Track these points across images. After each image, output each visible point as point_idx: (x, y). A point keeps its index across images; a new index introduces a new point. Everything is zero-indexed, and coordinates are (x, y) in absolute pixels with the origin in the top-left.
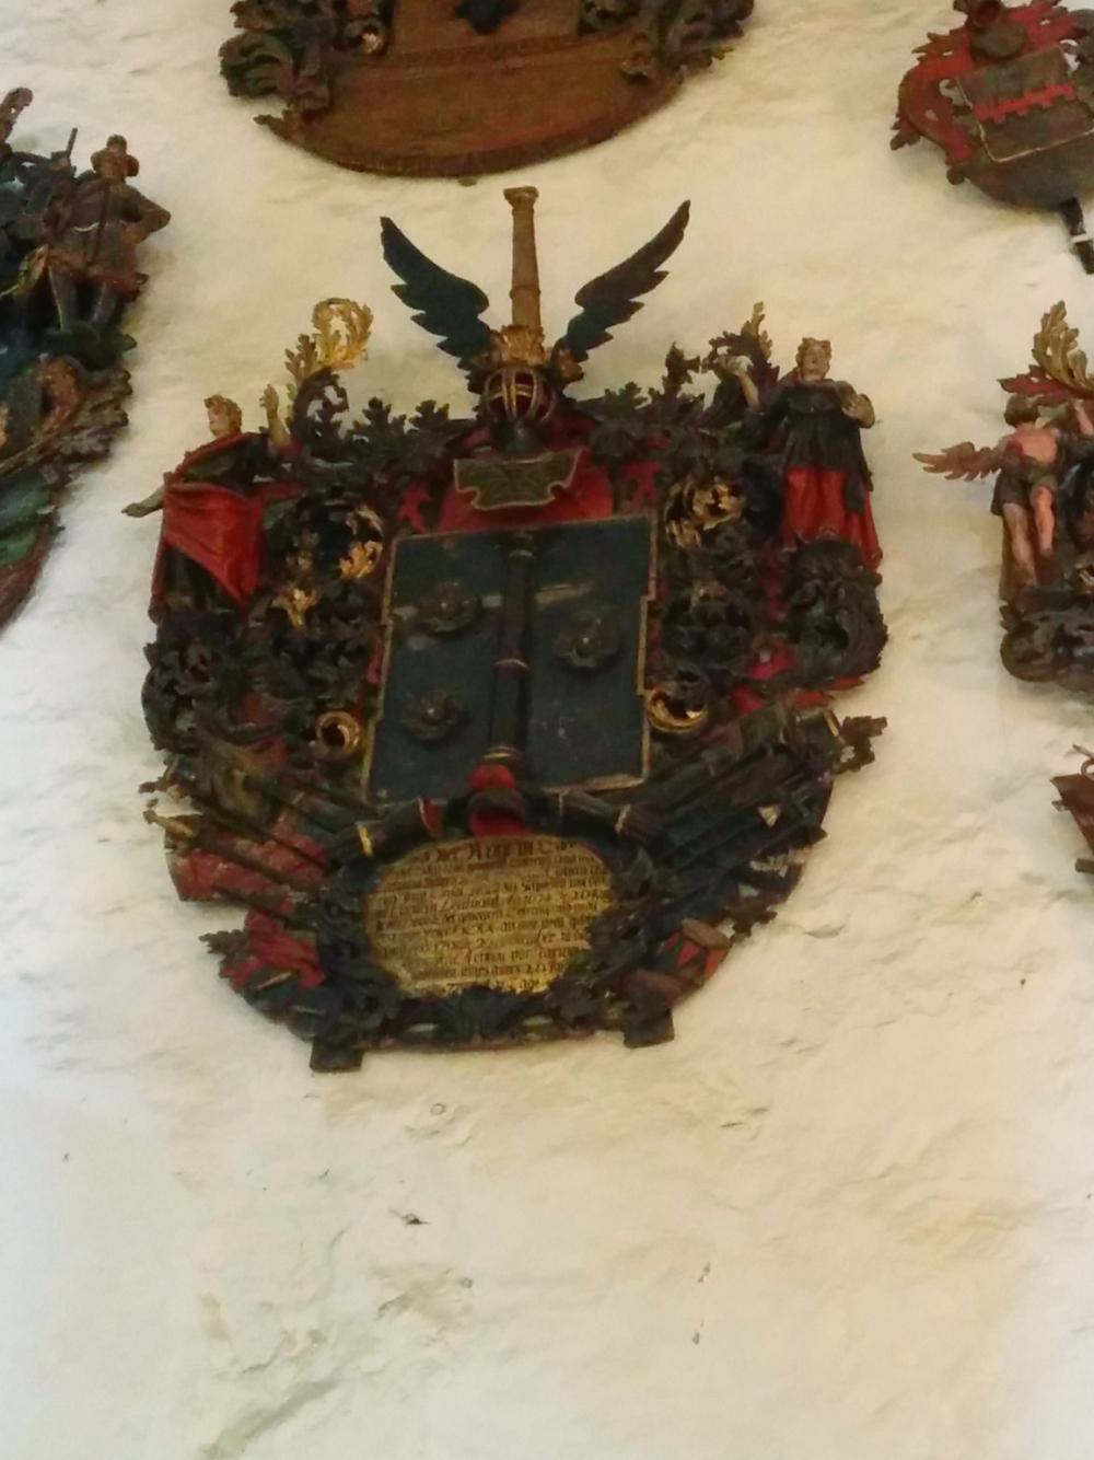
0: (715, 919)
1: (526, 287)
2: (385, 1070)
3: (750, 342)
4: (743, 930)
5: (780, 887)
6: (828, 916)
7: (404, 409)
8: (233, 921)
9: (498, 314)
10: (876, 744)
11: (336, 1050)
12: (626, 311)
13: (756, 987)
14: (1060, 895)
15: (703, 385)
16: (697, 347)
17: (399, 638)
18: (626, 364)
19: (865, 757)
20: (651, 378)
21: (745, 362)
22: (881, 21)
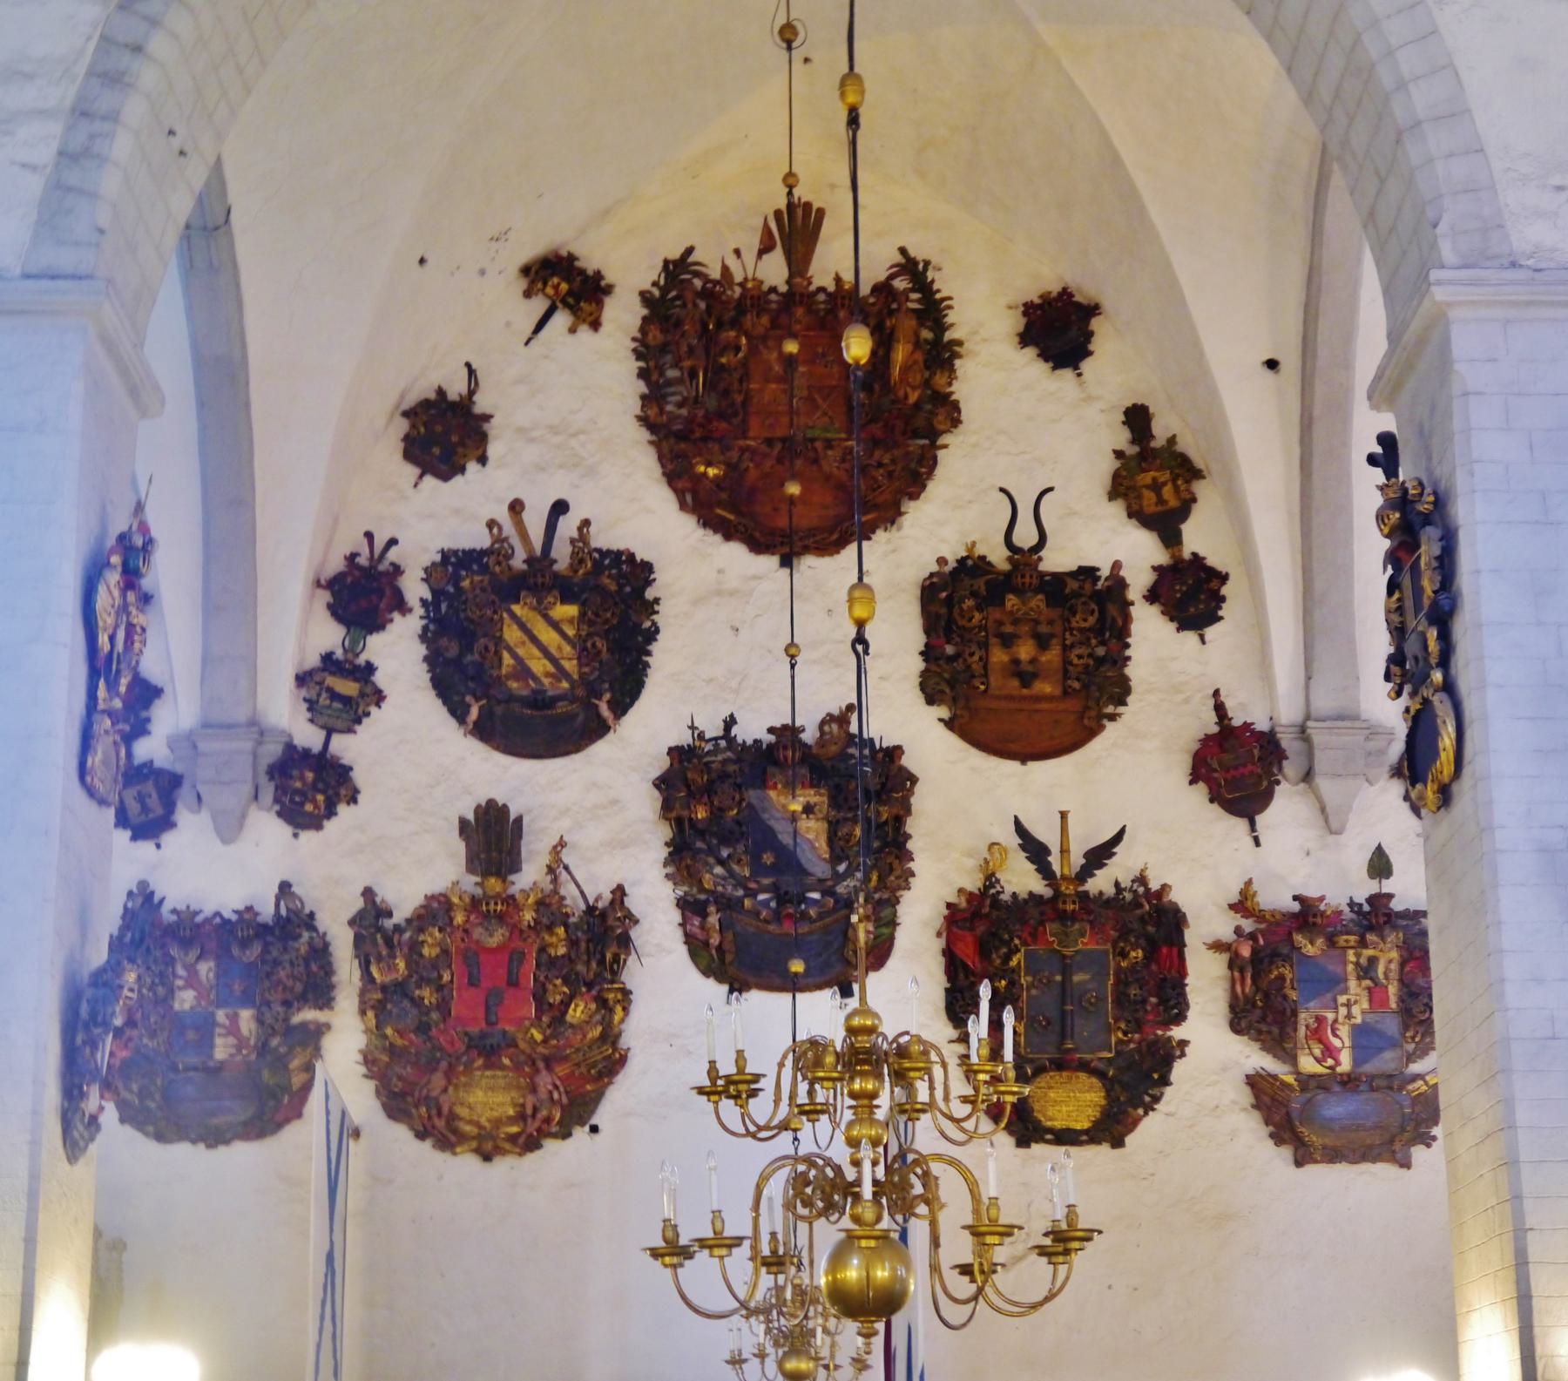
0: (1136, 1108)
1: (1064, 851)
2: (1037, 1149)
3: (1142, 880)
4: (1146, 1113)
5: (1157, 1099)
6: (1172, 1109)
7: (1023, 895)
9: (1054, 860)
10: (1187, 1050)
11: (1023, 1142)
12: (1101, 866)
13: (1149, 1131)
14: (1245, 1109)
15: (1128, 896)
16: (1126, 883)
17: (1028, 989)
18: (1101, 883)
19: (1183, 1055)
20: (1110, 891)
21: (1141, 890)
22: (1180, 697)
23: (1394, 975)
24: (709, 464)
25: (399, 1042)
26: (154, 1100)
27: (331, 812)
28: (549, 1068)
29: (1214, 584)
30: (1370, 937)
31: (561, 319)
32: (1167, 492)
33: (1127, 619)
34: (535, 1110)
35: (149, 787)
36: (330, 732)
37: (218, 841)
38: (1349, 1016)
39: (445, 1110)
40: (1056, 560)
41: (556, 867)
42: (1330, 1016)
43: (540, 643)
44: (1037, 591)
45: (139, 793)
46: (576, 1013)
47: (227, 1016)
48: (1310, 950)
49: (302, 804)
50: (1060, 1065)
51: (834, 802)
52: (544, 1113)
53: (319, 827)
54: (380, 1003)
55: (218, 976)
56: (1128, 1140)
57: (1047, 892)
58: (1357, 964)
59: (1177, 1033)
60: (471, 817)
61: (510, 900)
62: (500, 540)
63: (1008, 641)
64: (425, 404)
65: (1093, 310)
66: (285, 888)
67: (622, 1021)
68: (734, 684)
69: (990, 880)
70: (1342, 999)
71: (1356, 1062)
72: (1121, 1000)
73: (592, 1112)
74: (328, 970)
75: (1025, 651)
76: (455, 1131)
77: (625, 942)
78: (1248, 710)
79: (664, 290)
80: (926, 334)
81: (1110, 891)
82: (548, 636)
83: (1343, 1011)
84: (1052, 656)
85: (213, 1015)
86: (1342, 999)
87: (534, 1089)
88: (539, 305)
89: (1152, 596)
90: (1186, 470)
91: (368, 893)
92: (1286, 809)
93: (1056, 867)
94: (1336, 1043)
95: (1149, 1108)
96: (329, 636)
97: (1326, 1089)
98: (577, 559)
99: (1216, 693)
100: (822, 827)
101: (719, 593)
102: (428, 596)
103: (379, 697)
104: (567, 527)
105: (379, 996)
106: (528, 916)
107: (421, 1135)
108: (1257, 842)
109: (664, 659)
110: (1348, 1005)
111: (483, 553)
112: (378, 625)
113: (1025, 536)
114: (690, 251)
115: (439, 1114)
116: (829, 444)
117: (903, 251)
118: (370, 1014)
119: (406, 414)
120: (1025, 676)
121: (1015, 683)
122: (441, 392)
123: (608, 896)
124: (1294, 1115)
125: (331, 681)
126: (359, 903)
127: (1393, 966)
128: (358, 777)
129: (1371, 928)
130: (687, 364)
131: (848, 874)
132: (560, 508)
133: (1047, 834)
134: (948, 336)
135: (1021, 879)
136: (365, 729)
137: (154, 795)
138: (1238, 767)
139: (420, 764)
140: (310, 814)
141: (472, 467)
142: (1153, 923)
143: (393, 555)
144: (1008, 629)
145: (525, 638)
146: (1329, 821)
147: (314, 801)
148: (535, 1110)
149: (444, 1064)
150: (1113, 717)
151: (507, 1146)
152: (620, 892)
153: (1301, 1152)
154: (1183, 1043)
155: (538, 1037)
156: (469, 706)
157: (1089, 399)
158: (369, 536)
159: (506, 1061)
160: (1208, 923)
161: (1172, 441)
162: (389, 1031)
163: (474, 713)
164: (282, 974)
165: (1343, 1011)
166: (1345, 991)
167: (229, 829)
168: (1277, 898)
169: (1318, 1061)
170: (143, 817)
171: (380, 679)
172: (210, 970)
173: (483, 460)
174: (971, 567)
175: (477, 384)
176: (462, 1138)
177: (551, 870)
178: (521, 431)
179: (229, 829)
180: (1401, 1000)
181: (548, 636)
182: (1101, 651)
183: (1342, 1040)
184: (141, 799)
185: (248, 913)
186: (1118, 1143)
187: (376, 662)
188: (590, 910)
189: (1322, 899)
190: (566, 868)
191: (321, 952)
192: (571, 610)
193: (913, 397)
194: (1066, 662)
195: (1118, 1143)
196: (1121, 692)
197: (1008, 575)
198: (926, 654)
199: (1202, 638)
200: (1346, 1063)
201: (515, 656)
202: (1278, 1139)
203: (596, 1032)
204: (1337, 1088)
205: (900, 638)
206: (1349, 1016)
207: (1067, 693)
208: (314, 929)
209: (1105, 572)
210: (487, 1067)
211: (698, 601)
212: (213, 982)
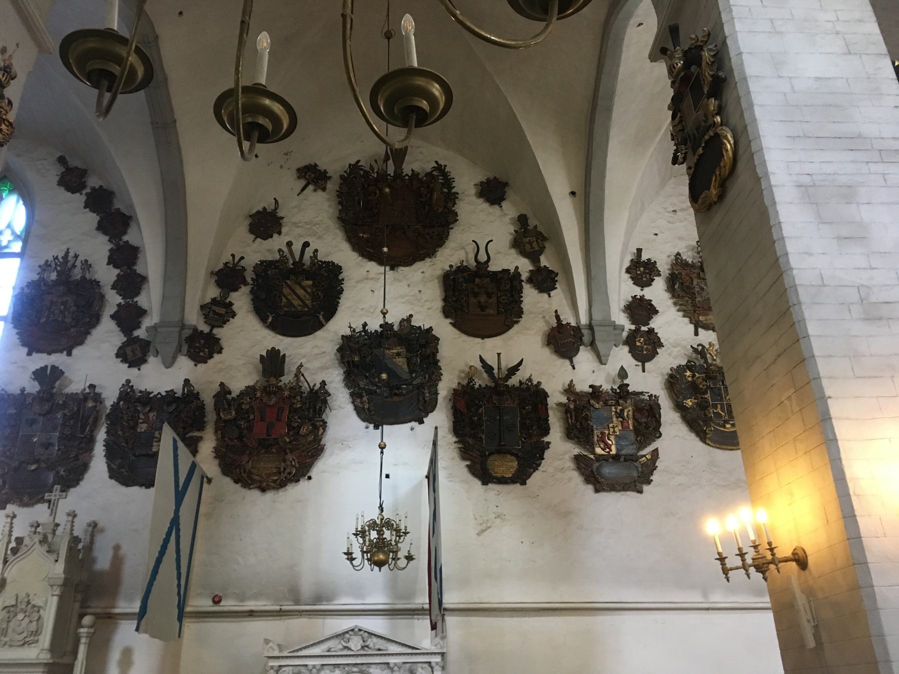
1: (499, 368)
2: (490, 486)
3: (530, 380)
5: (539, 465)
8: (468, 463)
9: (496, 371)
11: (485, 483)
13: (536, 478)
18: (514, 381)
20: (517, 385)
23: (631, 416)
24: (364, 233)
25: (230, 443)
27: (211, 357)
28: (291, 452)
29: (553, 276)
30: (621, 401)
31: (311, 187)
32: (535, 245)
33: (522, 287)
34: (285, 469)
35: (137, 346)
36: (213, 327)
38: (614, 432)
39: (247, 470)
40: (494, 267)
41: (299, 373)
42: (607, 432)
43: (298, 295)
44: (487, 277)
46: (303, 431)
48: (597, 406)
50: (499, 452)
51: (408, 350)
52: (288, 470)
53: (206, 362)
54: (222, 428)
55: (157, 418)
56: (528, 482)
57: (493, 385)
58: (616, 412)
59: (546, 439)
60: (264, 354)
61: (280, 389)
63: (476, 295)
64: (258, 212)
65: (506, 184)
66: (187, 382)
67: (322, 434)
68: (372, 310)
69: (471, 380)
70: (611, 425)
71: (617, 449)
72: (523, 425)
73: (308, 471)
74: (203, 415)
75: (483, 299)
76: (251, 479)
77: (325, 402)
78: (568, 318)
79: (349, 175)
80: (446, 190)
81: (517, 385)
82: (300, 292)
83: (611, 430)
84: (494, 300)
86: (611, 425)
87: (284, 461)
88: (303, 183)
89: (530, 280)
90: (541, 238)
91: (222, 385)
92: (584, 357)
93: (496, 375)
94: (610, 442)
95: (536, 469)
96: (214, 292)
97: (607, 460)
98: (313, 263)
99: (556, 311)
100: (404, 360)
101: (367, 279)
102: (254, 277)
103: (234, 315)
104: (309, 252)
106: (286, 393)
107: (236, 482)
108: (574, 368)
109: (346, 302)
110: (613, 427)
111: (277, 261)
112: (236, 290)
113: (483, 258)
114: (358, 161)
115: (245, 472)
116: (409, 226)
117: (436, 162)
118: (219, 432)
119: (251, 216)
120: (483, 308)
121: (479, 310)
122: (264, 208)
123: (318, 386)
124: (595, 470)
125: (214, 308)
126: (218, 388)
127: (631, 413)
128: (223, 343)
129: (621, 398)
130: (357, 198)
131: (416, 378)
132: (306, 245)
133: (492, 362)
134: (453, 191)
135: (482, 381)
136: (226, 327)
138: (564, 340)
139: (247, 339)
141: (275, 236)
142: (534, 396)
143: (243, 263)
144: (476, 290)
146: (601, 360)
147: (204, 351)
148: (285, 469)
149: (248, 452)
150: (517, 322)
151: (272, 484)
152: (323, 383)
153: (598, 486)
154: (549, 443)
155: (288, 440)
157: (505, 215)
158: (233, 255)
159: (274, 450)
160: (556, 397)
161: (536, 227)
162: (226, 439)
163: (270, 320)
164: (182, 416)
165: (611, 430)
166: (612, 422)
167: (169, 363)
168: (582, 387)
169: (603, 450)
171: (234, 308)
173: (280, 233)
174: (462, 269)
176: (254, 481)
177: (296, 376)
178: (295, 223)
179: (169, 363)
180: (634, 426)
181: (300, 292)
182: (511, 299)
183: (612, 441)
184: (133, 351)
185: (171, 393)
186: (523, 483)
187: (233, 302)
188: (312, 390)
189: (601, 386)
190: (303, 375)
191: (202, 407)
192: (310, 282)
193: (440, 210)
194: (498, 302)
195: (523, 483)
196: (520, 313)
197: (476, 272)
198: (445, 300)
199: (550, 296)
200: (614, 452)
201: (287, 299)
202: (588, 480)
203: (311, 438)
204: (610, 460)
205: (434, 295)
206: (614, 432)
207: (499, 313)
208: (199, 399)
209: (512, 271)
210: (266, 453)
211: (358, 282)
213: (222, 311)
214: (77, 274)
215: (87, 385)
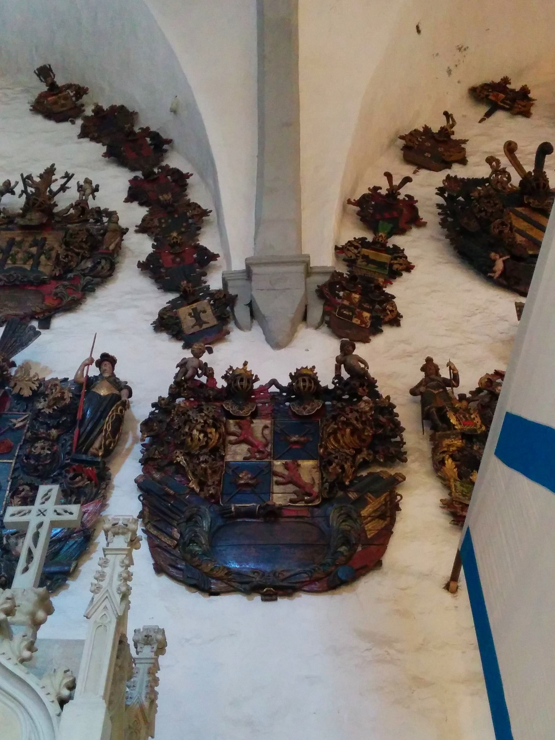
26: (200, 545)
27: (376, 330)
37: (268, 347)
45: (194, 310)
47: (286, 466)
49: (350, 318)
62: (498, 171)
85: (270, 465)
103: (409, 268)
105: (458, 443)
125: (365, 251)
137: (209, 311)
140: (358, 326)
145: (532, 227)
147: (360, 316)
156: (494, 261)
163: (499, 265)
170: (197, 328)
172: (266, 427)
175: (453, 121)
184: (196, 314)
208: (377, 395)
212: (269, 438)
213: (385, 258)
214: (65, 201)
215: (97, 356)
